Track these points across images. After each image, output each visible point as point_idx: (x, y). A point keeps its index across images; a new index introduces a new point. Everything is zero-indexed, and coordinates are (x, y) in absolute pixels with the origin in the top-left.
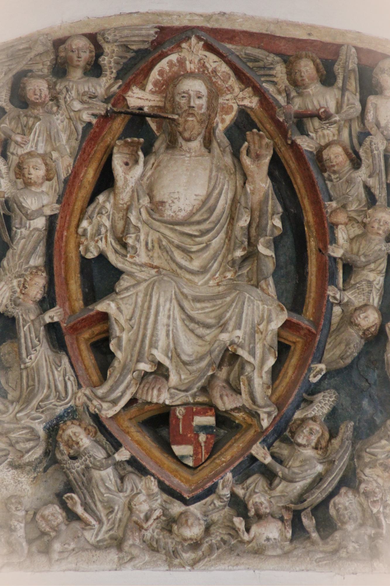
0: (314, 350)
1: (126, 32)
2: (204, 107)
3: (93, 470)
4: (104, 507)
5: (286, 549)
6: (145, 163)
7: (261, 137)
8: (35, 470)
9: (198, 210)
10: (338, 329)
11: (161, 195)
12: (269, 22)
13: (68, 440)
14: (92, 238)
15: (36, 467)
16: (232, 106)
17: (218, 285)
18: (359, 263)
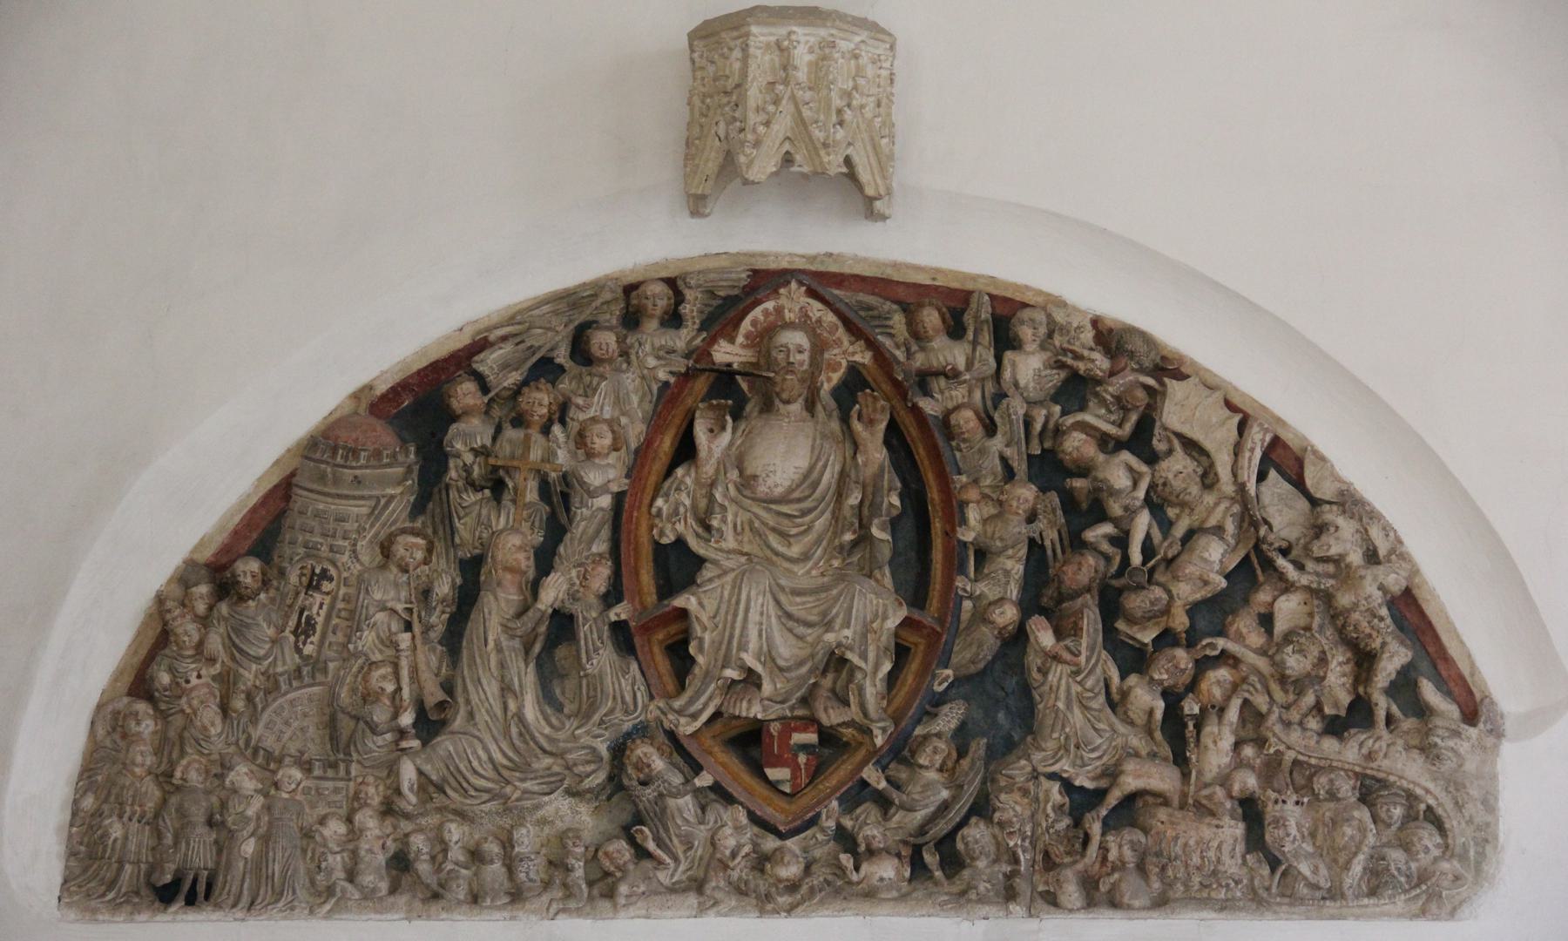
0: (939, 653)
1: (712, 276)
2: (807, 363)
4: (681, 842)
5: (904, 890)
6: (734, 430)
7: (875, 398)
9: (798, 486)
10: (967, 628)
14: (669, 520)
15: (598, 794)
16: (840, 364)
17: (822, 575)
18: (993, 549)
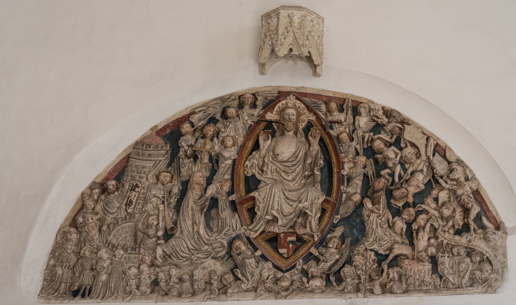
2: (295, 119)
3: (246, 259)
4: (250, 274)
5: (323, 290)
8: (222, 260)
9: (291, 157)
10: (345, 202)
11: (277, 151)
12: (320, 90)
13: (236, 247)
15: (223, 259)
16: (305, 120)
18: (353, 177)
